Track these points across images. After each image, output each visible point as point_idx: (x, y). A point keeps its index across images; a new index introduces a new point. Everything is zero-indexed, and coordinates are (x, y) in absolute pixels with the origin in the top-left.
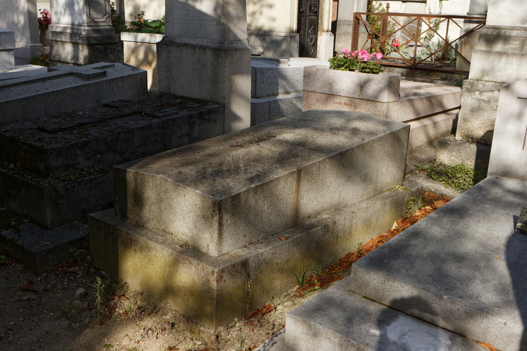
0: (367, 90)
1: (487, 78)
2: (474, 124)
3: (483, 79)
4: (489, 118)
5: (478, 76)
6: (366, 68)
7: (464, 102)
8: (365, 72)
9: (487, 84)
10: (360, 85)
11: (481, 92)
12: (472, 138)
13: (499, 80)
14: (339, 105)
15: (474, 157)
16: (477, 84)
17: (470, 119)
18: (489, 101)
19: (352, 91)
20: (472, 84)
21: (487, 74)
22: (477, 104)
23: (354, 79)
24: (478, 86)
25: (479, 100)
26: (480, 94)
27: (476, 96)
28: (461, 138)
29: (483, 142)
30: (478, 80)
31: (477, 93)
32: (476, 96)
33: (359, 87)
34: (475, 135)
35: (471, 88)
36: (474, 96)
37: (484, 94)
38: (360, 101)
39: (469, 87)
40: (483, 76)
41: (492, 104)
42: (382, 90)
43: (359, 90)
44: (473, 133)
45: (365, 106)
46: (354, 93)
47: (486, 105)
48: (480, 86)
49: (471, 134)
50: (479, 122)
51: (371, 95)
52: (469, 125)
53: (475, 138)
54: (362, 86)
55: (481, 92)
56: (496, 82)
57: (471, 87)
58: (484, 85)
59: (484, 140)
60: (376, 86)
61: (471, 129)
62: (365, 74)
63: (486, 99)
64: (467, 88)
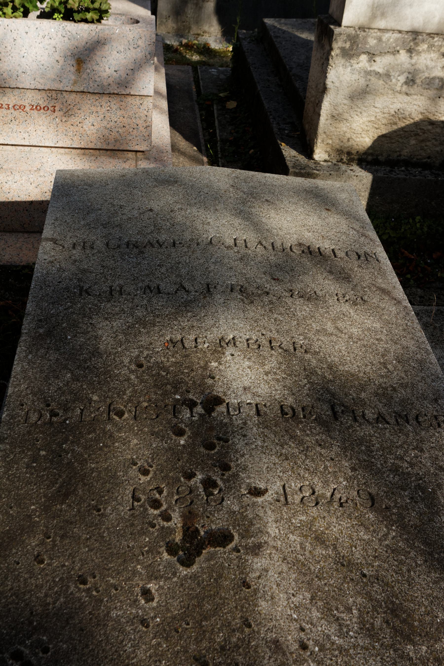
0: (96, 68)
1: (382, 24)
2: (354, 126)
3: (373, 26)
4: (386, 110)
5: (362, 20)
6: (88, 10)
7: (335, 80)
8: (86, 21)
9: (386, 36)
10: (73, 55)
11: (372, 56)
12: (349, 153)
13: (406, 26)
14: (16, 113)
15: (368, 191)
16: (365, 38)
17: (346, 116)
18: (388, 75)
19: (51, 74)
20: (353, 40)
21: (383, 15)
22: (362, 82)
23: (53, 42)
24: (366, 43)
25: (368, 73)
26: (369, 61)
27: (361, 65)
28: (326, 157)
29: (370, 158)
30: (362, 28)
31: (364, 58)
32: (361, 65)
33: (73, 62)
34: (355, 147)
35: (351, 48)
36: (356, 66)
37: (377, 59)
38: (78, 97)
39: (348, 45)
40: (373, 17)
41: (394, 80)
42: (140, 66)
43: (73, 69)
44: (350, 143)
45: (94, 109)
46: (59, 78)
47: (381, 82)
48: (372, 42)
49: (347, 145)
50: (365, 119)
51: (110, 80)
52: (343, 127)
53: (354, 152)
54: (82, 57)
55: (372, 56)
56: (400, 32)
57: (352, 45)
58: (380, 40)
59: (372, 154)
60: (121, 57)
61: (348, 135)
62: (83, 26)
63: (381, 71)
64: (343, 49)
